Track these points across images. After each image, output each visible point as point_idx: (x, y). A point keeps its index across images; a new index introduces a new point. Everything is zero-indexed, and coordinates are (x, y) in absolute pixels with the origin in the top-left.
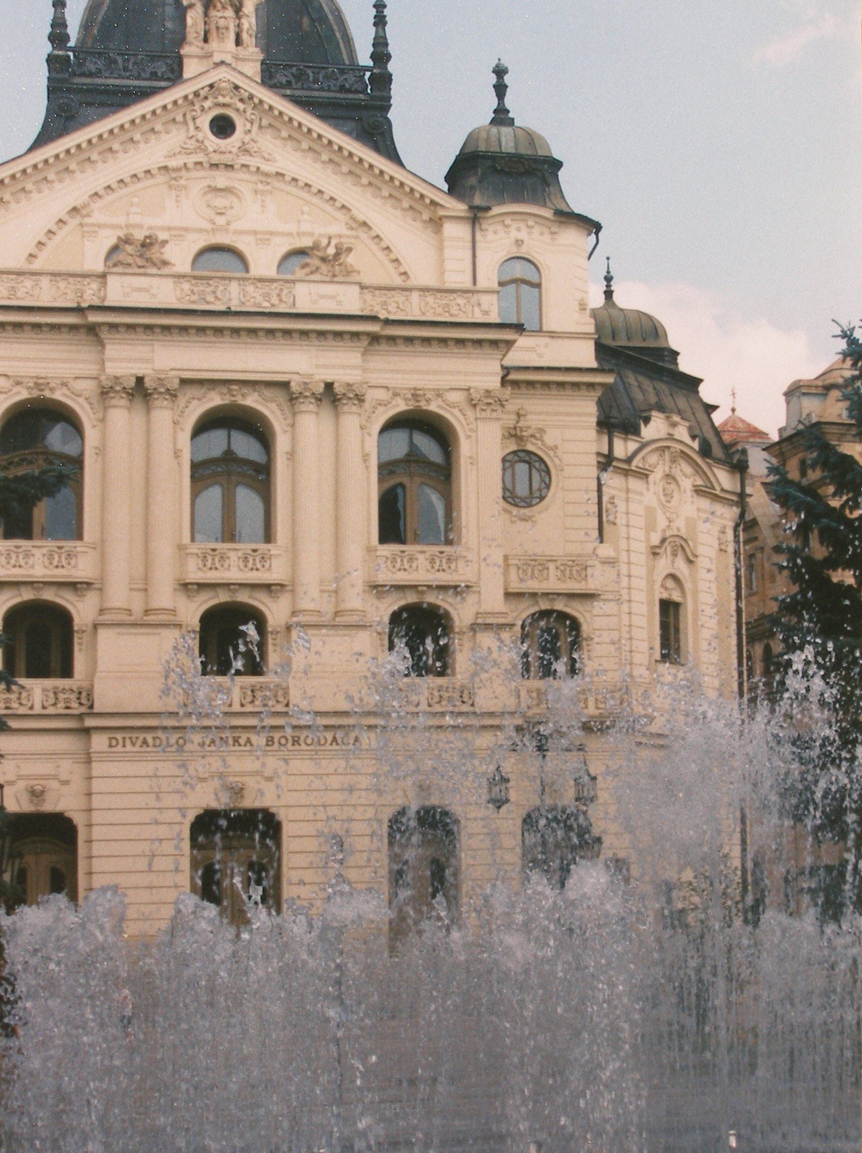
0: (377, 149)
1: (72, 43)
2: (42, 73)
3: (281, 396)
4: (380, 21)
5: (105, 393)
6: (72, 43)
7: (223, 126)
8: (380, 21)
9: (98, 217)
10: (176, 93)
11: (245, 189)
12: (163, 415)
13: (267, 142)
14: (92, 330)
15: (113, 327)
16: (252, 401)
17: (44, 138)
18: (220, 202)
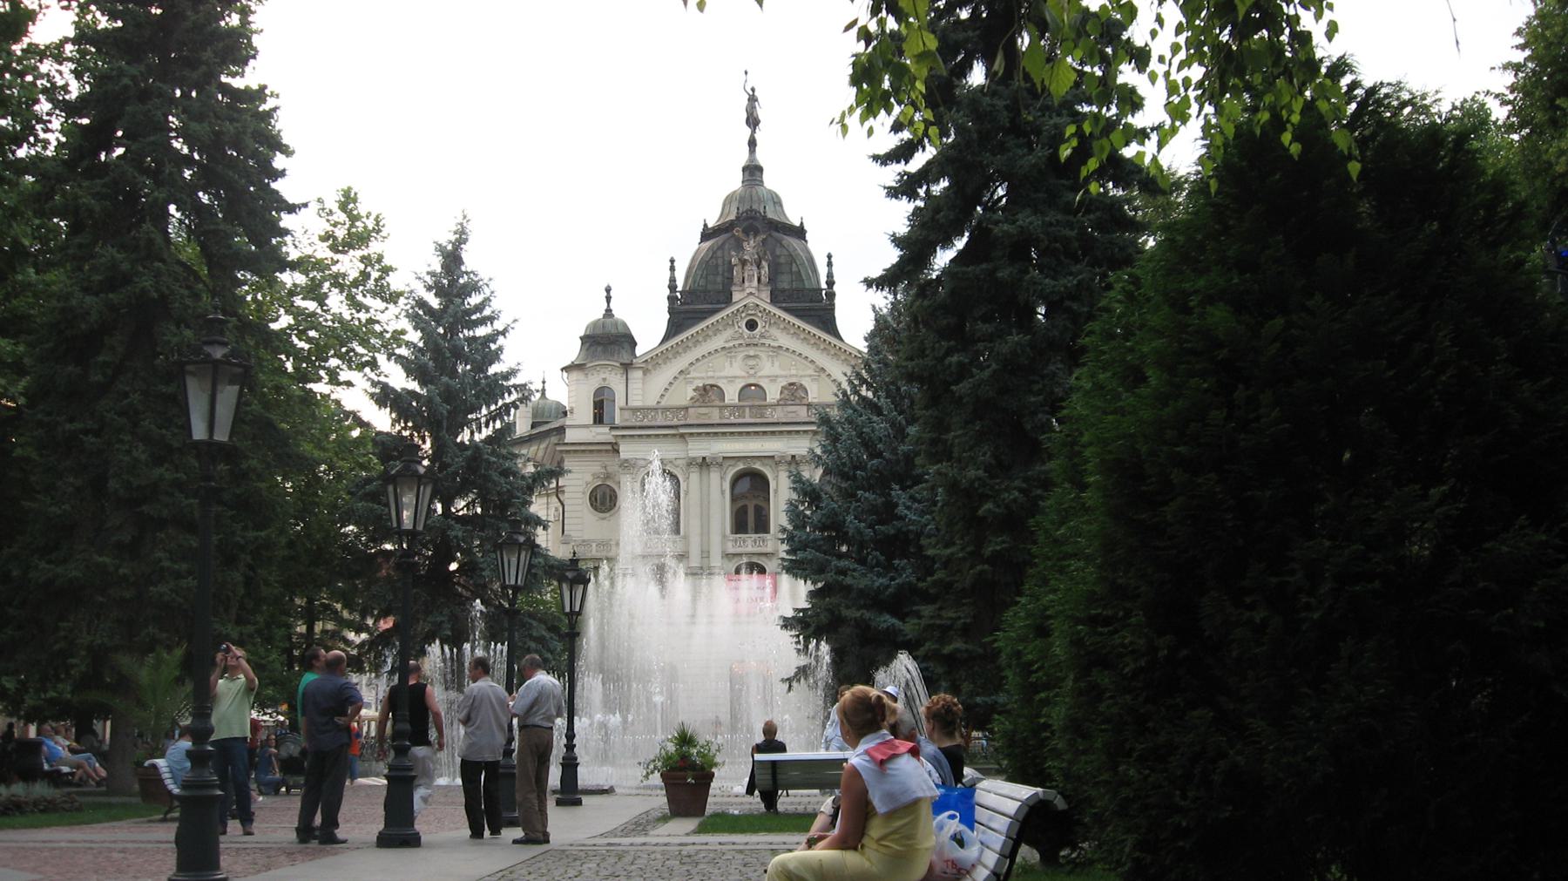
0: (828, 332)
1: (680, 288)
2: (664, 304)
3: (770, 462)
4: (830, 264)
5: (689, 465)
6: (680, 288)
7: (752, 325)
8: (830, 264)
9: (693, 374)
10: (729, 311)
11: (763, 355)
12: (715, 476)
13: (774, 332)
14: (682, 436)
15: (691, 434)
16: (758, 466)
17: (666, 338)
18: (752, 362)
